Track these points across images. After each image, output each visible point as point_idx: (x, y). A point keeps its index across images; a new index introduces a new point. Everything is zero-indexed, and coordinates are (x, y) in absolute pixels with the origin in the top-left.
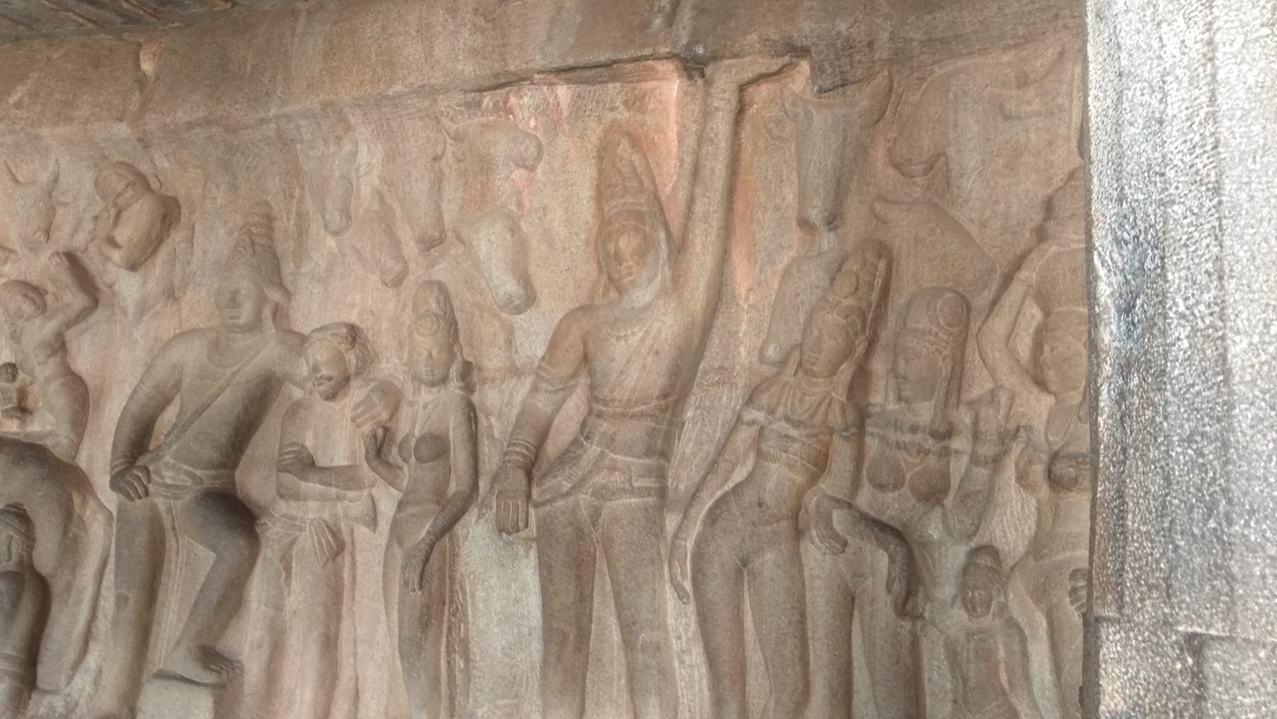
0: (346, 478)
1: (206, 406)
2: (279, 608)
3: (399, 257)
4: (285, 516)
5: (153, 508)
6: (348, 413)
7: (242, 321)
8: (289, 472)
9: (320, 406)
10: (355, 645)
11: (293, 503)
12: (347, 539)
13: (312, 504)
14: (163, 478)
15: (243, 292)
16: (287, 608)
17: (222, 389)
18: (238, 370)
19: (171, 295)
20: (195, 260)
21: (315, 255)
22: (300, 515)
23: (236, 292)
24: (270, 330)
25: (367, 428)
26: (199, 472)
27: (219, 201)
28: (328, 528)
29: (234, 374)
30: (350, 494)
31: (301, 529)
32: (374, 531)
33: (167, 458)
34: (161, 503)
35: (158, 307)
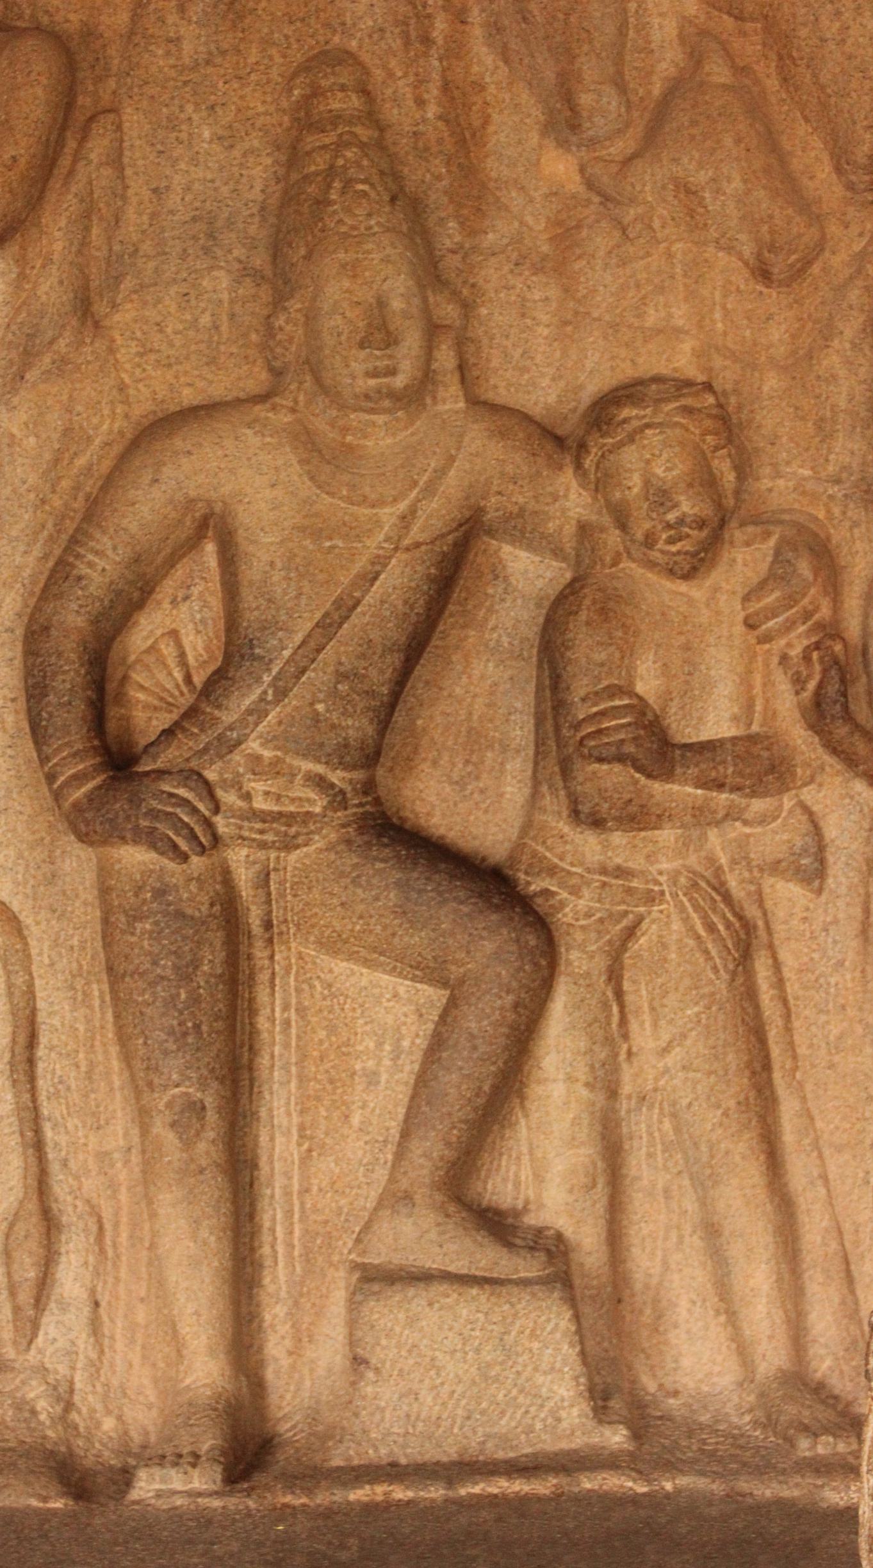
0: (755, 765)
1: (346, 607)
2: (613, 1093)
3: (807, 208)
4: (604, 871)
5: (226, 877)
6: (733, 609)
7: (399, 381)
8: (621, 759)
9: (660, 592)
10: (820, 1156)
11: (618, 838)
12: (752, 912)
13: (667, 835)
14: (247, 797)
15: (397, 304)
16: (627, 1088)
17: (381, 562)
18: (413, 511)
19: (85, 309)
20: (130, 214)
21: (515, 199)
22: (636, 863)
23: (381, 303)
24: (450, 400)
25: (798, 641)
26: (337, 777)
27: (187, 47)
28: (714, 889)
29: (406, 520)
30: (758, 805)
31: (651, 898)
32: (819, 892)
33: (253, 745)
34: (241, 862)
35: (62, 345)
